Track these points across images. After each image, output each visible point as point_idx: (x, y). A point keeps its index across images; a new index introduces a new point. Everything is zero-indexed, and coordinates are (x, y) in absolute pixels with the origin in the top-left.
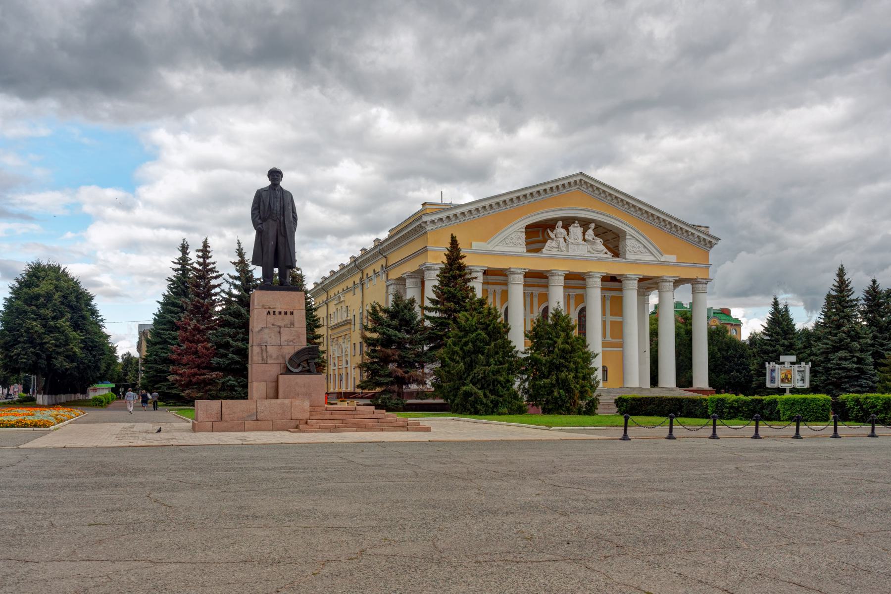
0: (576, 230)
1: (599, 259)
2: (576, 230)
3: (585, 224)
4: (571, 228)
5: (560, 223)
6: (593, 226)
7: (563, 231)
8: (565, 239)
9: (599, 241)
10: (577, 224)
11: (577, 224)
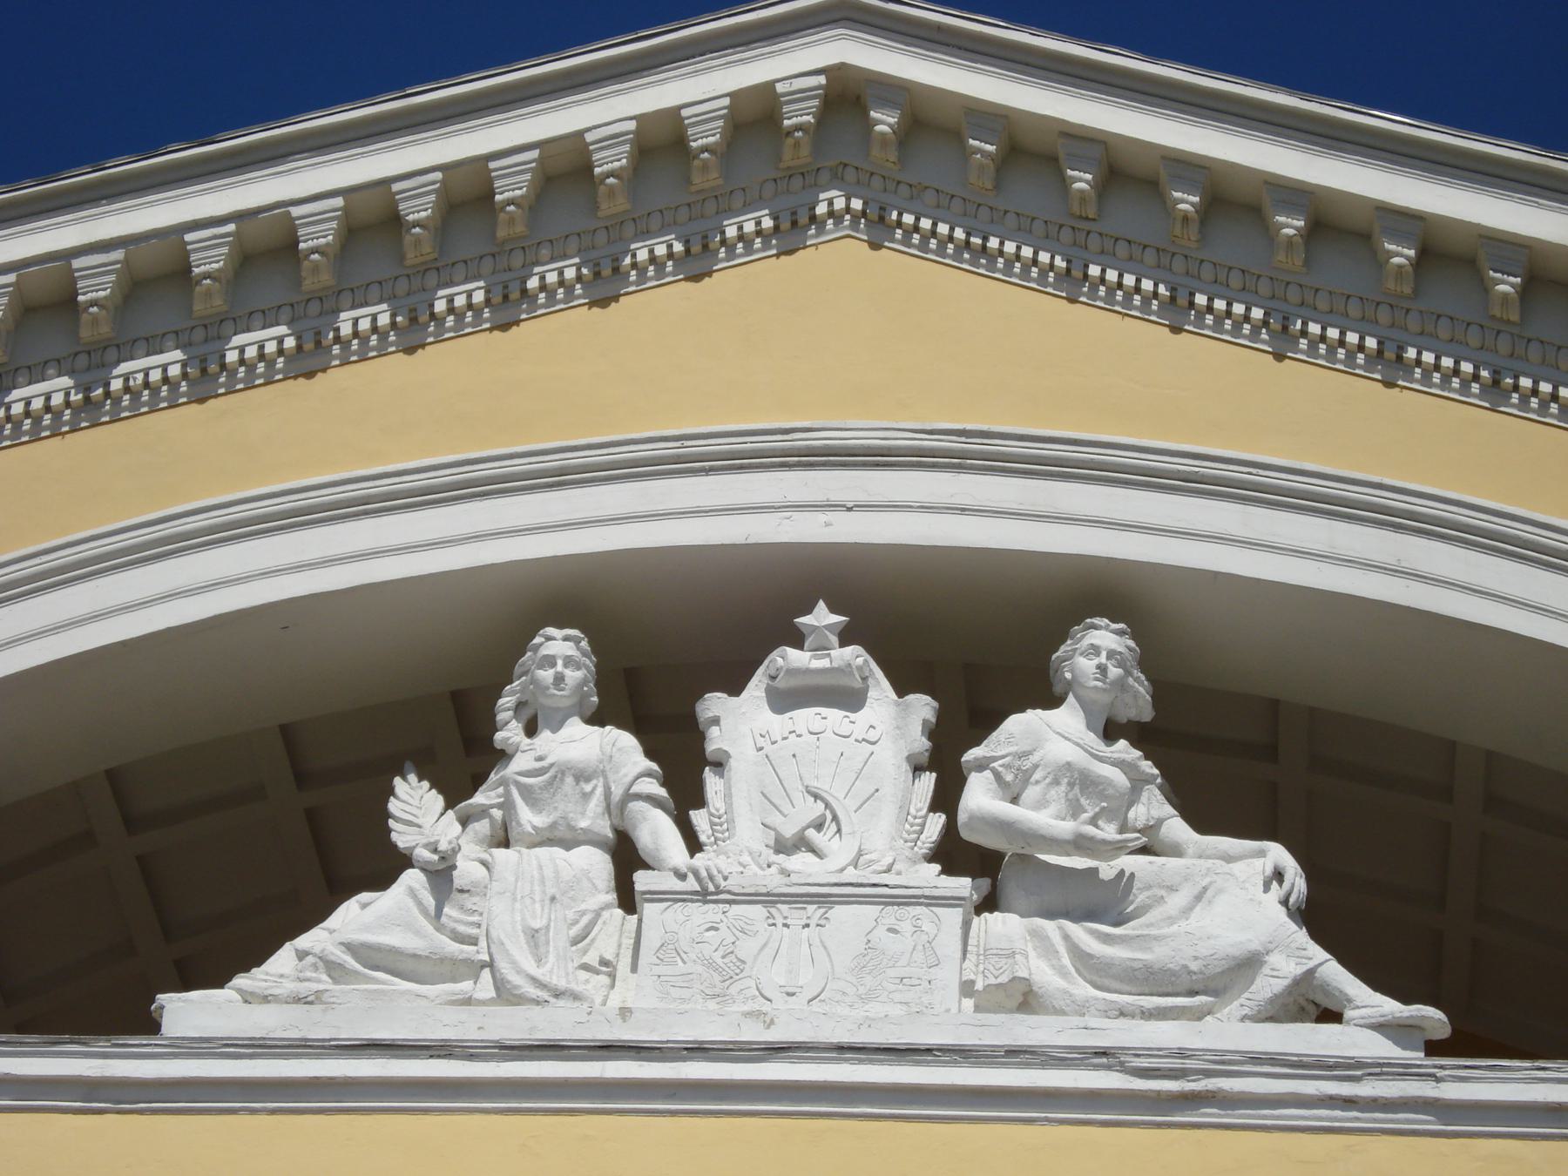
0: (822, 755)
1: (1176, 1098)
2: (822, 755)
3: (964, 651)
4: (737, 722)
5: (561, 655)
6: (1097, 651)
7: (621, 753)
8: (627, 857)
9: (1237, 897)
10: (823, 647)
11: (823, 647)
